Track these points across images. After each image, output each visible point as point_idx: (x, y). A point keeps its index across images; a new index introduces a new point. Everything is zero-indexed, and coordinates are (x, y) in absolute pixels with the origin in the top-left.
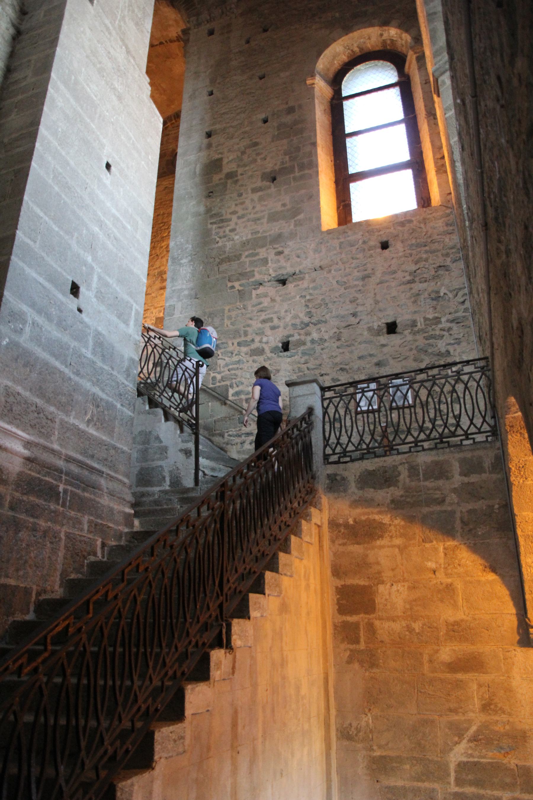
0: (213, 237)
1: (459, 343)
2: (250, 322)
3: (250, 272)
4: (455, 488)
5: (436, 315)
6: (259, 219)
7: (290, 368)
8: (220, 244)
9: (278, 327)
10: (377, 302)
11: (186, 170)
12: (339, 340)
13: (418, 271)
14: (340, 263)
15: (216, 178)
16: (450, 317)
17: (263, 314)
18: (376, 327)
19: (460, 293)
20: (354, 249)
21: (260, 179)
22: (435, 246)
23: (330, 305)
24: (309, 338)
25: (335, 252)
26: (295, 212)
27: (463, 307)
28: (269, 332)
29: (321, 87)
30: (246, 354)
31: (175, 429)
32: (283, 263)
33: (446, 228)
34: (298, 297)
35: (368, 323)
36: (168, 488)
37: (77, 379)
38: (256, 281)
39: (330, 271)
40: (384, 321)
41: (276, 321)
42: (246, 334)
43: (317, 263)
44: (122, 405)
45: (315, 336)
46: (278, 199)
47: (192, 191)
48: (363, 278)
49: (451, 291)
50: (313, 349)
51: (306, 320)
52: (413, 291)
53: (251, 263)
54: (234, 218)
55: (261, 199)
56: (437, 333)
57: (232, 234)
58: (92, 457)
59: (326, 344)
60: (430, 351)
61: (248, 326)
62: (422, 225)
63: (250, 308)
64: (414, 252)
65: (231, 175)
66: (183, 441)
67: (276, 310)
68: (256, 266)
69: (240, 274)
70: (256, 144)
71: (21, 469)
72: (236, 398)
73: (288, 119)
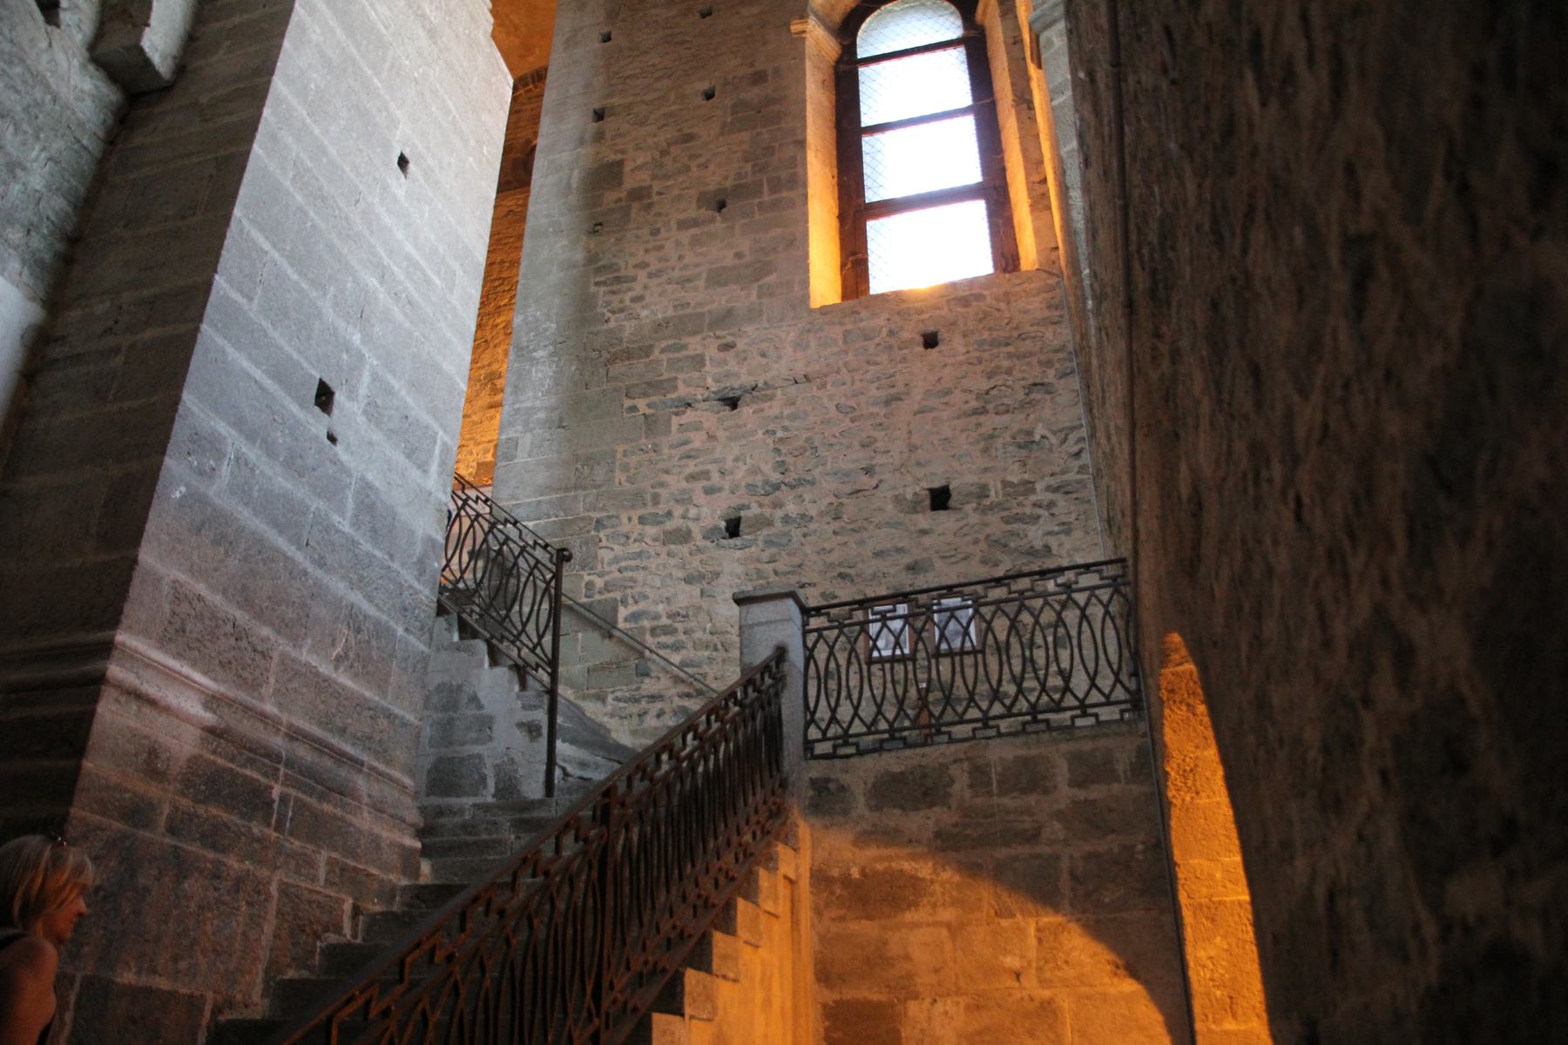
0: (599, 310)
1: (1068, 532)
2: (665, 478)
3: (668, 380)
4: (1060, 811)
5: (1026, 476)
6: (689, 280)
7: (740, 569)
8: (612, 325)
9: (720, 490)
10: (913, 449)
11: (551, 179)
12: (837, 518)
13: (994, 392)
14: (844, 370)
15: (610, 197)
16: (1053, 482)
17: (692, 463)
18: (909, 497)
19: (1073, 437)
20: (871, 345)
21: (694, 206)
22: (1028, 345)
23: (822, 452)
24: (779, 513)
25: (835, 349)
26: (760, 270)
27: (1077, 463)
28: (700, 498)
29: (818, 39)
30: (655, 540)
31: (510, 682)
32: (733, 365)
33: (1047, 313)
34: (760, 432)
35: (895, 488)
36: (490, 799)
37: (319, 573)
38: (679, 399)
39: (824, 386)
40: (925, 485)
41: (715, 476)
42: (656, 500)
43: (800, 369)
44: (406, 630)
45: (792, 509)
46: (729, 244)
47: (562, 219)
48: (887, 403)
49: (1054, 433)
50: (787, 534)
51: (775, 477)
52: (982, 430)
53: (672, 363)
54: (642, 275)
55: (695, 241)
56: (1028, 510)
57: (637, 306)
58: (342, 731)
59: (812, 526)
60: (1012, 545)
61: (662, 485)
62: (1002, 306)
63: (666, 451)
64: (986, 355)
65: (638, 194)
66: (524, 707)
67: (717, 455)
68: (681, 370)
69: (648, 384)
70: (689, 138)
71: (196, 751)
72: (633, 625)
73: (753, 94)
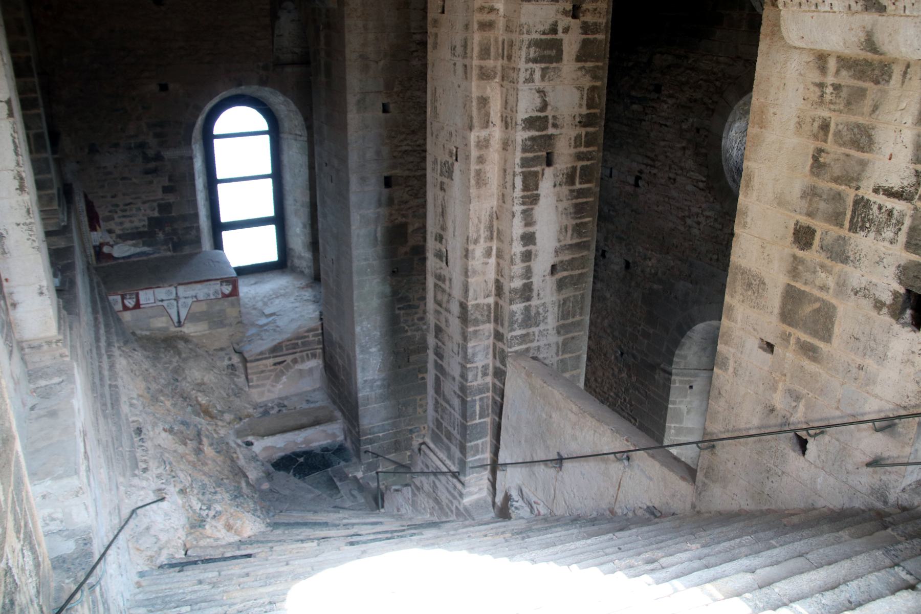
0: (402, 325)
8: (409, 334)
11: (363, 231)
47: (374, 263)
57: (421, 323)
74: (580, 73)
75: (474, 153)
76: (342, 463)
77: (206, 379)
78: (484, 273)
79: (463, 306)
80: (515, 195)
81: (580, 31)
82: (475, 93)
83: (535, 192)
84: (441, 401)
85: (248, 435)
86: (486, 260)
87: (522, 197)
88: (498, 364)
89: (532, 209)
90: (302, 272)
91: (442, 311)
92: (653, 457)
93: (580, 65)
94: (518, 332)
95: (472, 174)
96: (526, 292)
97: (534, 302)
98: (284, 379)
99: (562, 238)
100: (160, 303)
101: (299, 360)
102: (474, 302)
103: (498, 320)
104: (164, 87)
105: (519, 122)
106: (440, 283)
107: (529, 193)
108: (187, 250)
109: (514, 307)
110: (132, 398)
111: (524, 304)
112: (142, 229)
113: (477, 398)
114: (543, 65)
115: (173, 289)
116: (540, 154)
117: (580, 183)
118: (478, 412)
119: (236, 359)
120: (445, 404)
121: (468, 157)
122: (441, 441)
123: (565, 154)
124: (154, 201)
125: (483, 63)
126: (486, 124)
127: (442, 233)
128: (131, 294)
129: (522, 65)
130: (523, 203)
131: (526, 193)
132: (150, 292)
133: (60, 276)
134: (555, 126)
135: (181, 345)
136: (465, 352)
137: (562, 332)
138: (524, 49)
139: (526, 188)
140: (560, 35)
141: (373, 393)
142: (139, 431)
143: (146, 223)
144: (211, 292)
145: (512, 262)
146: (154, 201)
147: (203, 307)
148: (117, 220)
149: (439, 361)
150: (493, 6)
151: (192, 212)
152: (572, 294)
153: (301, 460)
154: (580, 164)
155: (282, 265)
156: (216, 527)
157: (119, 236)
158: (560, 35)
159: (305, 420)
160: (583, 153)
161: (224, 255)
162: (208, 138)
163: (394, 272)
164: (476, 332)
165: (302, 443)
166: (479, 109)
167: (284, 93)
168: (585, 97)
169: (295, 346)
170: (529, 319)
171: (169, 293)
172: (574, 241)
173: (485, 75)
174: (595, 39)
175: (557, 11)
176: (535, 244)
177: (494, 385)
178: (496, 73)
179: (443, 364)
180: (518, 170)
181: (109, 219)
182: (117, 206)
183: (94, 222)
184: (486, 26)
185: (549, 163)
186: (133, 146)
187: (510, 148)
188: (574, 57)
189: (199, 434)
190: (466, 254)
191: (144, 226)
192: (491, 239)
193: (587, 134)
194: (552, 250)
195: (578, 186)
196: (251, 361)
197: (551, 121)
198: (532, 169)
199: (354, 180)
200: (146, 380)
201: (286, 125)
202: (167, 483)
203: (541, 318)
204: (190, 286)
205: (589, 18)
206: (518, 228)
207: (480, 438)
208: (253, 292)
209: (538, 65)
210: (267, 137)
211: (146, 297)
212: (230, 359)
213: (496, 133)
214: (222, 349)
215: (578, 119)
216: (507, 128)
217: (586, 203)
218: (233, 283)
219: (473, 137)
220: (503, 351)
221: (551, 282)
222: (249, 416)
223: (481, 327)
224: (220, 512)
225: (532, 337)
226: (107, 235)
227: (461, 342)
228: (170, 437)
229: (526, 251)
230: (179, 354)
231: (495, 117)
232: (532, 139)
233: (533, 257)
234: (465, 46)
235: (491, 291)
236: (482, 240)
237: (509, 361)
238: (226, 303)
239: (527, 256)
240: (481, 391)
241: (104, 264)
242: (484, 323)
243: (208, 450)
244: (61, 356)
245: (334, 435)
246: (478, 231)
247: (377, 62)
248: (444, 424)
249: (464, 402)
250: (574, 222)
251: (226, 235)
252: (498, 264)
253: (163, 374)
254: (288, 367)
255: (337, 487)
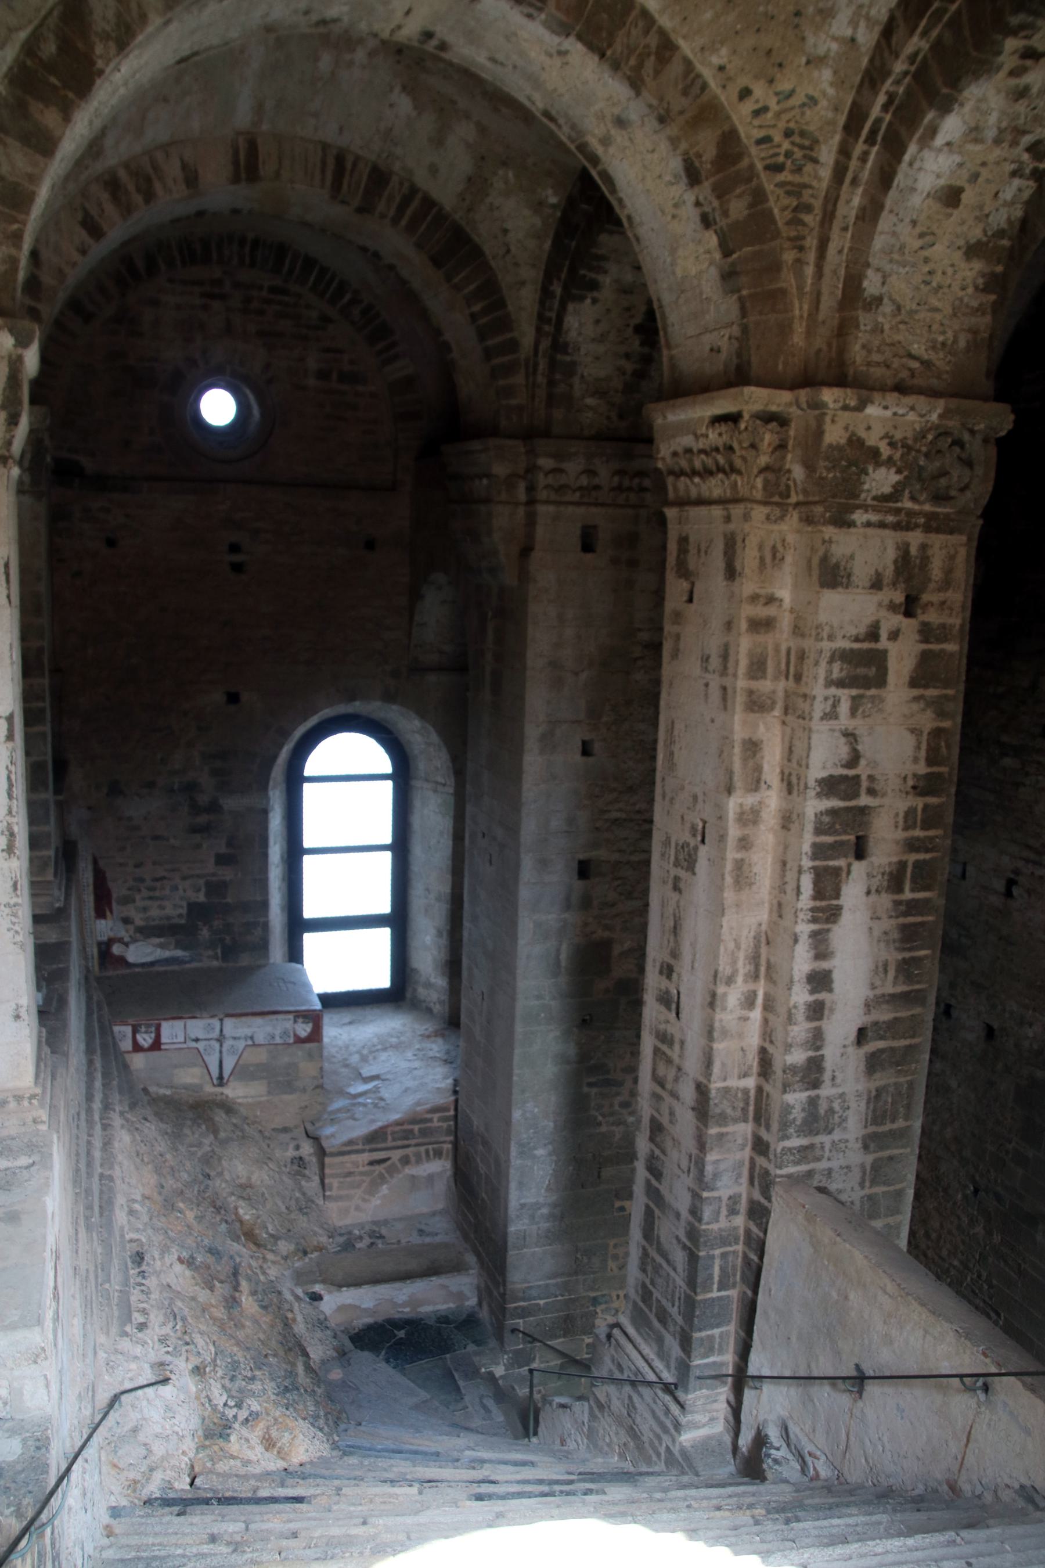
0: (593, 1113)
8: (604, 1129)
47: (553, 1003)
57: (624, 1111)
74: (915, 707)
75: (734, 832)
76: (471, 1348)
77: (255, 1178)
78: (741, 1035)
79: (702, 1090)
80: (800, 905)
81: (917, 637)
82: (739, 733)
83: (835, 902)
84: (653, 1253)
85: (315, 1282)
86: (745, 1013)
87: (813, 910)
88: (757, 1196)
89: (828, 930)
90: (429, 1011)
91: (664, 1094)
92: (1033, 1389)
93: (916, 692)
94: (795, 1142)
95: (729, 866)
96: (812, 1073)
97: (826, 1091)
98: (384, 1189)
99: (878, 983)
100: (194, 1044)
101: (413, 1159)
102: (720, 1085)
103: (760, 1117)
104: (233, 698)
105: (812, 783)
106: (664, 1048)
107: (824, 903)
108: (245, 960)
109: (790, 1098)
110: (134, 1201)
111: (807, 1094)
112: (176, 921)
113: (717, 1252)
114: (854, 692)
115: (216, 1022)
116: (845, 838)
117: (912, 890)
118: (716, 1279)
119: (307, 1149)
120: (659, 1259)
121: (722, 838)
122: (649, 1325)
123: (887, 838)
124: (198, 876)
125: (755, 685)
126: (756, 783)
127: (672, 962)
128: (148, 1026)
129: (819, 690)
130: (814, 920)
131: (818, 904)
132: (179, 1024)
133: (44, 990)
134: (871, 792)
135: (220, 1117)
136: (701, 1171)
137: (872, 1146)
138: (823, 664)
139: (819, 894)
140: (884, 643)
141: (535, 1227)
142: (139, 1258)
143: (184, 911)
144: (278, 1032)
145: (790, 1019)
146: (198, 876)
147: (261, 1056)
148: (140, 903)
149: (654, 1182)
150: (773, 594)
151: (259, 898)
152: (893, 1080)
153: (401, 1334)
154: (913, 857)
155: (398, 994)
156: (247, 1440)
157: (140, 930)
158: (884, 643)
159: (413, 1265)
160: (918, 839)
161: (303, 973)
162: (295, 781)
163: (584, 1021)
164: (721, 1135)
165: (404, 1304)
166: (745, 760)
167: (422, 715)
168: (924, 746)
169: (408, 1135)
170: (815, 1120)
171: (210, 1028)
172: (901, 988)
173: (756, 705)
174: (942, 651)
175: (880, 605)
176: (830, 990)
177: (748, 1232)
178: (774, 703)
179: (661, 1188)
180: (807, 863)
181: (126, 901)
182: (142, 880)
183: (103, 904)
184: (761, 625)
185: (860, 852)
186: (176, 787)
187: (795, 827)
188: (907, 679)
189: (235, 1274)
190: (712, 1001)
191: (180, 916)
192: (756, 977)
193: (926, 807)
194: (859, 1002)
195: (908, 895)
196: (333, 1155)
197: (865, 784)
198: (831, 863)
199: (527, 862)
200: (158, 1171)
201: (421, 766)
202: (176, 1353)
203: (837, 1119)
204: (244, 1019)
205: (932, 617)
206: (802, 962)
207: (718, 1326)
208: (345, 1037)
209: (846, 691)
210: (389, 785)
211: (172, 1031)
212: (297, 1148)
213: (772, 800)
214: (286, 1130)
215: (910, 782)
216: (790, 793)
217: (922, 924)
218: (315, 1019)
219: (732, 805)
220: (767, 1173)
221: (856, 1057)
222: (320, 1248)
223: (729, 1129)
224: (257, 1414)
225: (818, 1153)
226: (120, 924)
227: (695, 1152)
228: (188, 1273)
229: (815, 1002)
230: (216, 1132)
231: (771, 773)
232: (833, 812)
233: (826, 1012)
234: (725, 656)
235: (750, 1067)
236: (740, 979)
237: (777, 1192)
238: (299, 1053)
239: (817, 1011)
240: (725, 1240)
241: (111, 973)
242: (735, 1121)
243: (247, 1302)
244: (35, 1121)
245: (460, 1296)
246: (734, 962)
247: (577, 674)
248: (656, 1294)
249: (693, 1259)
250: (900, 956)
251: (310, 940)
252: (766, 1021)
253: (188, 1164)
254: (392, 1171)
255: (458, 1389)
